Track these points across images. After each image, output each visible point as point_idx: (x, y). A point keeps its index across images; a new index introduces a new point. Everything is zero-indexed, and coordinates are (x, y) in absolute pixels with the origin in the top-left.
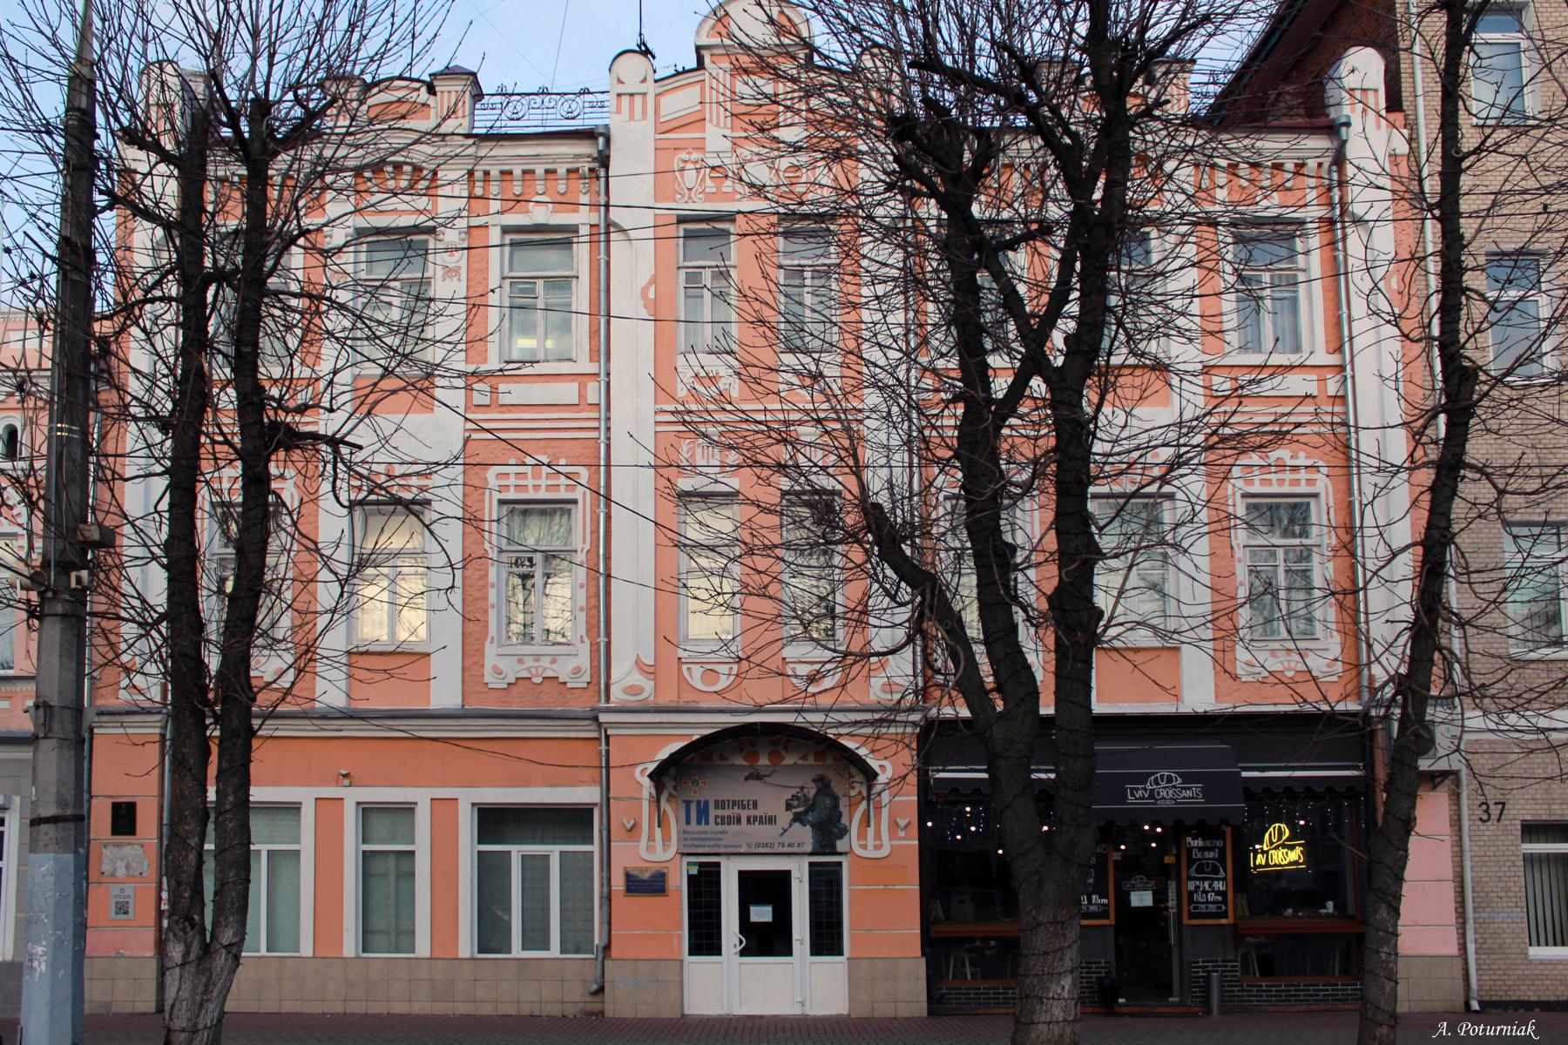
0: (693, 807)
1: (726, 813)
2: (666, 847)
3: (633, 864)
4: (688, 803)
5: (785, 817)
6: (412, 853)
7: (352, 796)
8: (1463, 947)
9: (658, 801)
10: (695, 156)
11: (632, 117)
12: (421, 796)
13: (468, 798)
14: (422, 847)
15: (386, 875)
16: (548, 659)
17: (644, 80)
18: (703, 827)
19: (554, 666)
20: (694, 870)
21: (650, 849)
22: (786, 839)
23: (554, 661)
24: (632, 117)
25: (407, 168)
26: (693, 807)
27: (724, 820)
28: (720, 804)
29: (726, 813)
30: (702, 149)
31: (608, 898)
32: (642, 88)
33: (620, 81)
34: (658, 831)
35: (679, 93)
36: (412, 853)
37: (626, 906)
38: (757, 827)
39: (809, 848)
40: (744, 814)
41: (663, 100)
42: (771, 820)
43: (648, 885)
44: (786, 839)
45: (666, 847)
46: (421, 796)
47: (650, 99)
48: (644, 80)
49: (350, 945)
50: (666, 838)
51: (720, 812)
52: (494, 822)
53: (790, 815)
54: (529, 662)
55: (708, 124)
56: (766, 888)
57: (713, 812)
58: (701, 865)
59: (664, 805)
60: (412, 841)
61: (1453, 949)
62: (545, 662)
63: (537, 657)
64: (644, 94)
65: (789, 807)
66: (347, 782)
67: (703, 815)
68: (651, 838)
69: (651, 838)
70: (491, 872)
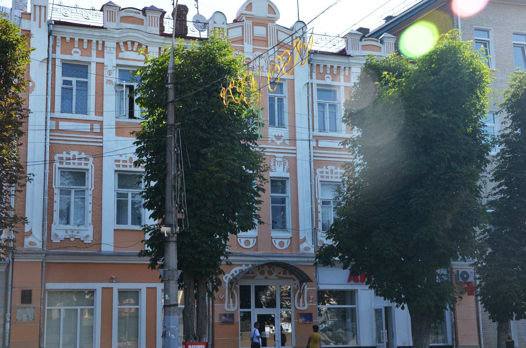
2: (234, 306)
8: (480, 343)
10: (240, 53)
17: (223, 23)
21: (229, 307)
25: (136, 44)
30: (243, 51)
32: (223, 26)
33: (215, 23)
34: (231, 300)
35: (235, 29)
41: (229, 31)
45: (234, 306)
47: (225, 30)
50: (234, 302)
55: (245, 42)
61: (478, 344)
68: (229, 303)
69: (229, 303)
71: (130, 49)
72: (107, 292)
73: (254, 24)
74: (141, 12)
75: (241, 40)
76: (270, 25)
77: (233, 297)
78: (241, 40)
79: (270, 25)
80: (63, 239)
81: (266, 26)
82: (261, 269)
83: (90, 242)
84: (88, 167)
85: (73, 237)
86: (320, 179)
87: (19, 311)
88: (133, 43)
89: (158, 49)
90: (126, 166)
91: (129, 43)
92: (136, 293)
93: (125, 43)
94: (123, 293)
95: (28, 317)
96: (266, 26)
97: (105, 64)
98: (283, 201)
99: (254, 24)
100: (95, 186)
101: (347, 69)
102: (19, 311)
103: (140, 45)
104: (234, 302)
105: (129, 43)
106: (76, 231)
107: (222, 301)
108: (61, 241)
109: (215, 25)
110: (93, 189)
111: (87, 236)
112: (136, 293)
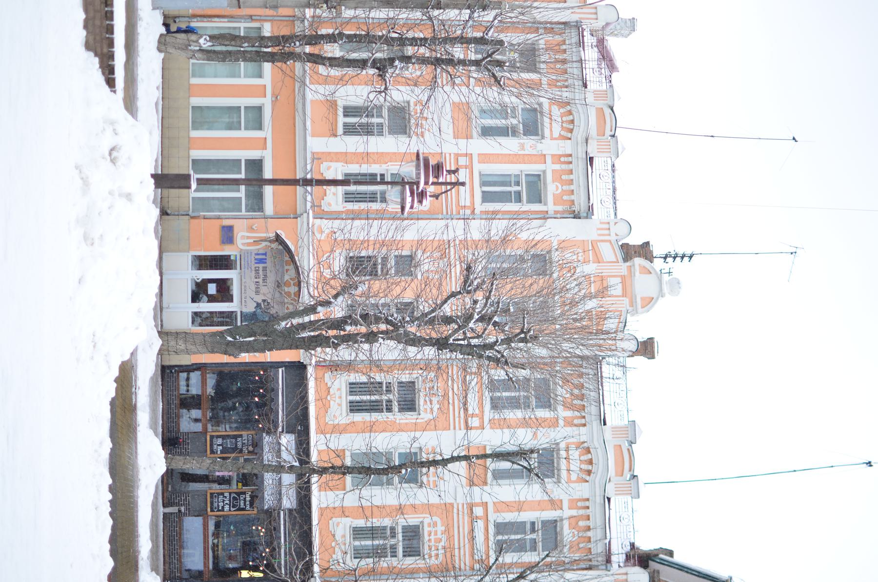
0: (264, 257)
1: (261, 272)
3: (235, 230)
4: (265, 254)
5: (259, 299)
6: (240, 129)
9: (265, 240)
11: (598, 229)
12: (267, 132)
14: (243, 133)
15: (230, 117)
17: (616, 235)
18: (253, 261)
20: (232, 258)
21: (243, 237)
22: (248, 300)
23: (334, 194)
24: (598, 229)
26: (264, 257)
27: (257, 271)
28: (265, 269)
29: (261, 272)
31: (219, 218)
32: (613, 234)
33: (616, 223)
34: (252, 241)
35: (612, 251)
36: (240, 129)
37: (217, 224)
38: (253, 287)
39: (244, 310)
40: (261, 280)
42: (257, 292)
43: (228, 235)
44: (248, 300)
45: (243, 244)
48: (616, 235)
49: (196, 101)
50: (249, 244)
51: (261, 269)
53: (260, 301)
56: (224, 291)
57: (261, 266)
58: (236, 260)
59: (264, 244)
60: (246, 129)
64: (609, 235)
65: (264, 301)
67: (261, 261)
68: (248, 238)
69: (248, 238)
71: (564, 119)
72: (261, 91)
73: (623, 278)
74: (612, 133)
75: (598, 260)
76: (626, 301)
77: (256, 242)
78: (598, 260)
79: (626, 301)
81: (624, 295)
82: (292, 282)
84: (423, 415)
86: (427, 521)
88: (572, 122)
89: (570, 153)
90: (430, 535)
91: (571, 118)
93: (570, 113)
94: (259, 109)
96: (624, 295)
97: (543, 141)
98: (389, 410)
99: (623, 278)
101: (583, 421)
103: (571, 131)
105: (571, 118)
107: (251, 229)
109: (612, 224)
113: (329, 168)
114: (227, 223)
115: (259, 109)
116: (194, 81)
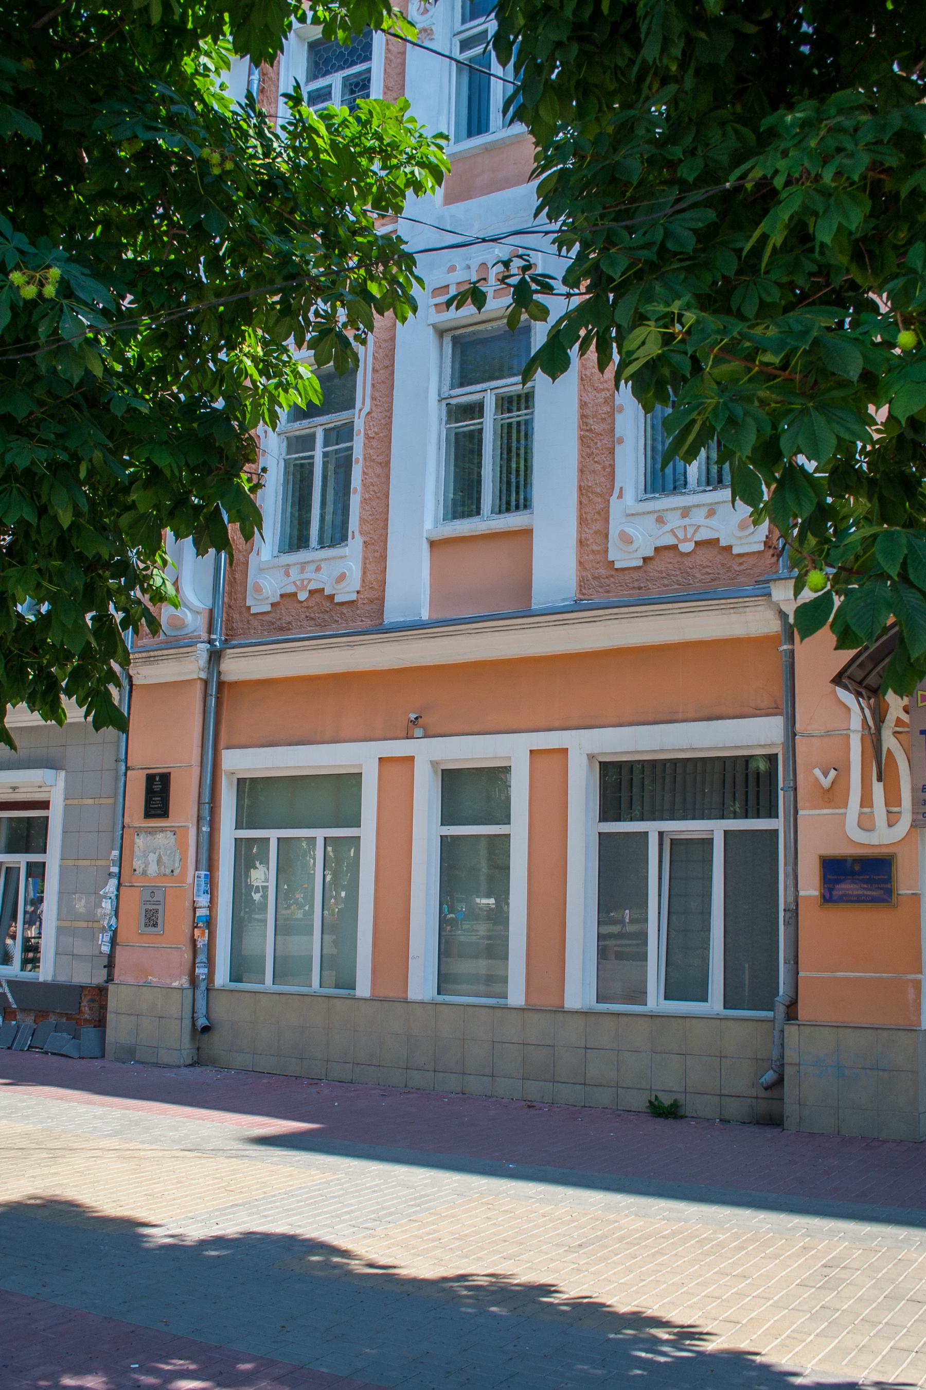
7: (430, 754)
13: (586, 747)
14: (518, 830)
15: (470, 870)
16: (704, 511)
19: (713, 522)
21: (866, 824)
23: (711, 513)
34: (878, 789)
46: (512, 750)
50: (893, 799)
52: (626, 787)
54: (674, 521)
60: (506, 820)
62: (698, 517)
63: (686, 512)
66: (418, 732)
68: (866, 800)
69: (866, 800)
70: (618, 867)
80: (277, 599)
83: (354, 597)
85: (303, 588)
87: (140, 842)
92: (497, 776)
94: (452, 780)
95: (159, 861)
100: (373, 398)
102: (140, 842)
104: (893, 799)
106: (312, 567)
107: (834, 795)
108: (272, 605)
110: (367, 408)
111: (342, 578)
112: (497, 776)
113: (627, 539)
114: (810, 888)
115: (452, 780)
116: (516, 996)
